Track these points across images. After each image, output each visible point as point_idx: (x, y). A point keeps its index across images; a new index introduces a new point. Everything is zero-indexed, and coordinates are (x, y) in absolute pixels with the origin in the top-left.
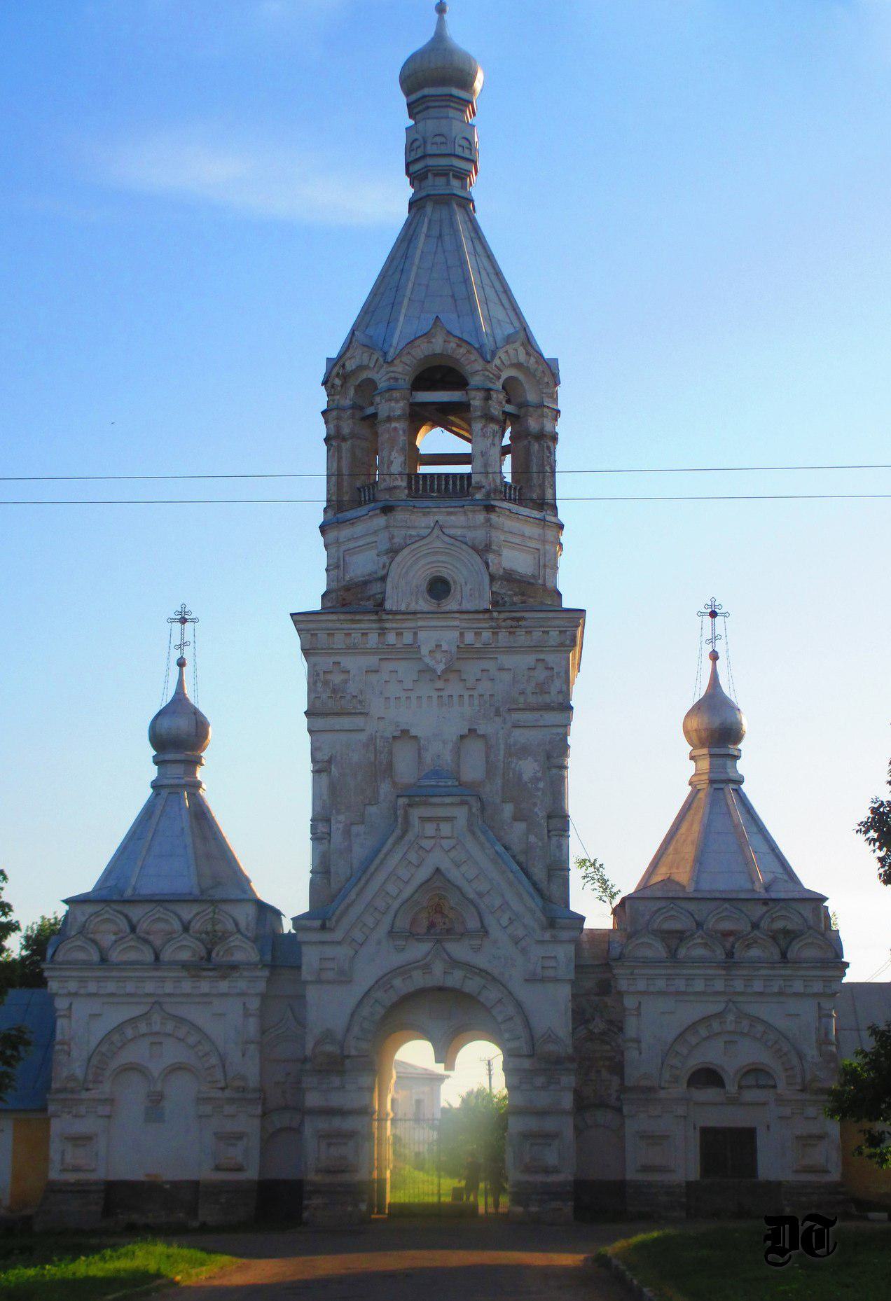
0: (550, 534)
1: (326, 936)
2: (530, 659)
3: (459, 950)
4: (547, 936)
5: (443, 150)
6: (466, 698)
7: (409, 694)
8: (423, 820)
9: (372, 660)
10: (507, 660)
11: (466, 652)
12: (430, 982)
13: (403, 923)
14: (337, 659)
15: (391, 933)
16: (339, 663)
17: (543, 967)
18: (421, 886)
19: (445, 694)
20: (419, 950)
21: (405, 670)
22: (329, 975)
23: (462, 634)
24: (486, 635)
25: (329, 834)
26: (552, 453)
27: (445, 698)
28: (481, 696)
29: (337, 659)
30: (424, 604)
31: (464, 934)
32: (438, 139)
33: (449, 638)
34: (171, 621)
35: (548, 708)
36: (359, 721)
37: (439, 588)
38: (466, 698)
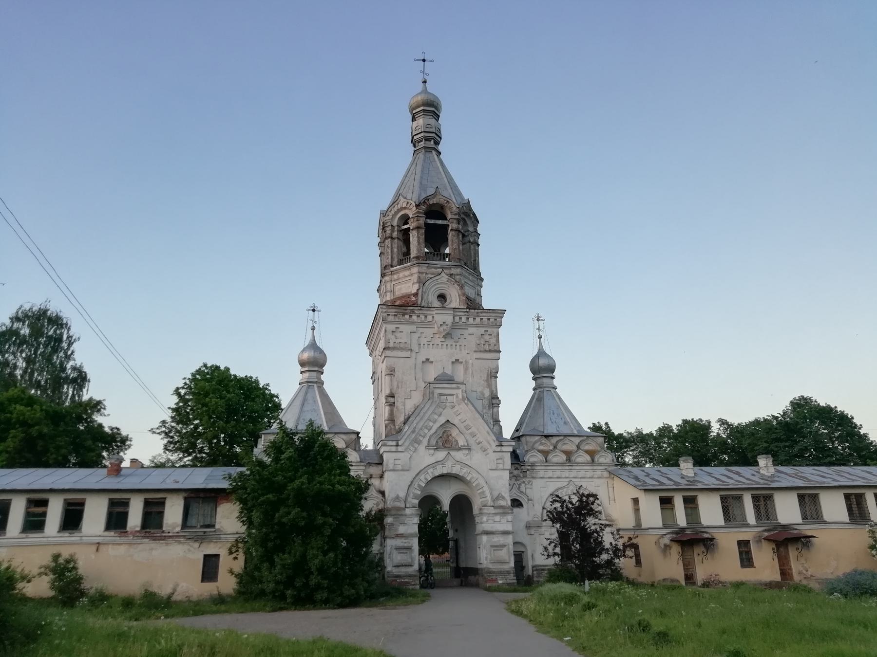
0: (480, 282)
1: (400, 449)
2: (482, 330)
3: (458, 455)
4: (499, 449)
5: (431, 130)
6: (454, 346)
7: (429, 343)
8: (441, 395)
9: (413, 328)
10: (471, 330)
11: (455, 326)
12: (445, 472)
13: (433, 442)
14: (398, 326)
15: (428, 447)
16: (399, 328)
17: (497, 463)
18: (441, 425)
19: (445, 344)
20: (441, 455)
21: (429, 332)
22: (399, 467)
23: (454, 318)
24: (464, 319)
25: (394, 403)
26: (477, 253)
27: (445, 346)
28: (460, 345)
29: (398, 326)
30: (436, 303)
31: (459, 449)
32: (428, 126)
33: (449, 319)
34: (309, 310)
35: (490, 351)
36: (407, 354)
37: (442, 297)
38: (454, 346)
